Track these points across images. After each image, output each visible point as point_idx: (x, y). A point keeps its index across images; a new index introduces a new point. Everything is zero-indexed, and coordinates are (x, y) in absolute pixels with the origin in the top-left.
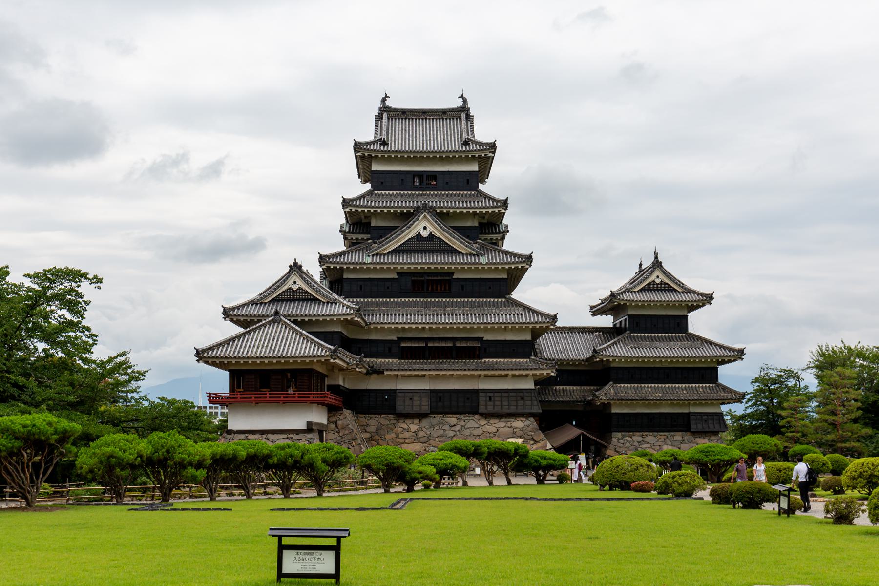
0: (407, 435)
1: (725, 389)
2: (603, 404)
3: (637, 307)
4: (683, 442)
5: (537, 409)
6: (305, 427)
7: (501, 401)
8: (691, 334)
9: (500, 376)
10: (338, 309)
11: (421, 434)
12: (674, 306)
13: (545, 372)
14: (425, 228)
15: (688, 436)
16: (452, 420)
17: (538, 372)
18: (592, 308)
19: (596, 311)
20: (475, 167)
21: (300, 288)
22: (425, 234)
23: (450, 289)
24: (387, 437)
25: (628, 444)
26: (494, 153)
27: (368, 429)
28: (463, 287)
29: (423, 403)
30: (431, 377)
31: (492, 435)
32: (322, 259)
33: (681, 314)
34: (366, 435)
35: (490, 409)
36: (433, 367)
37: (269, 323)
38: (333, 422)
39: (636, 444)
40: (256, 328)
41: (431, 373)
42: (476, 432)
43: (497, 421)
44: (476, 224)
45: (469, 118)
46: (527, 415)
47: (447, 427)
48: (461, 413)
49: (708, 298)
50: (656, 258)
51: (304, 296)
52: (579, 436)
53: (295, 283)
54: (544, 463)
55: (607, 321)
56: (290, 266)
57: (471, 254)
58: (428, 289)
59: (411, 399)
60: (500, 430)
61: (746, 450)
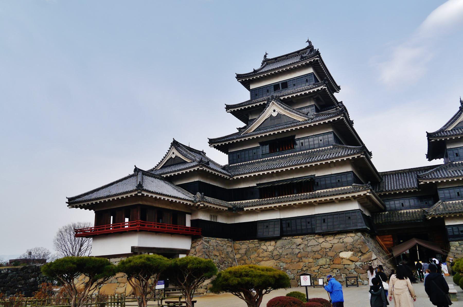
0: (265, 254)
2: (433, 218)
6: (129, 251)
7: (333, 222)
14: (274, 111)
16: (298, 240)
17: (356, 194)
21: (176, 156)
22: (275, 114)
26: (320, 57)
29: (276, 229)
31: (328, 250)
32: (212, 142)
34: (238, 256)
35: (324, 228)
41: (275, 205)
42: (315, 249)
43: (332, 238)
46: (356, 231)
47: (294, 246)
51: (180, 161)
52: (415, 246)
53: (173, 153)
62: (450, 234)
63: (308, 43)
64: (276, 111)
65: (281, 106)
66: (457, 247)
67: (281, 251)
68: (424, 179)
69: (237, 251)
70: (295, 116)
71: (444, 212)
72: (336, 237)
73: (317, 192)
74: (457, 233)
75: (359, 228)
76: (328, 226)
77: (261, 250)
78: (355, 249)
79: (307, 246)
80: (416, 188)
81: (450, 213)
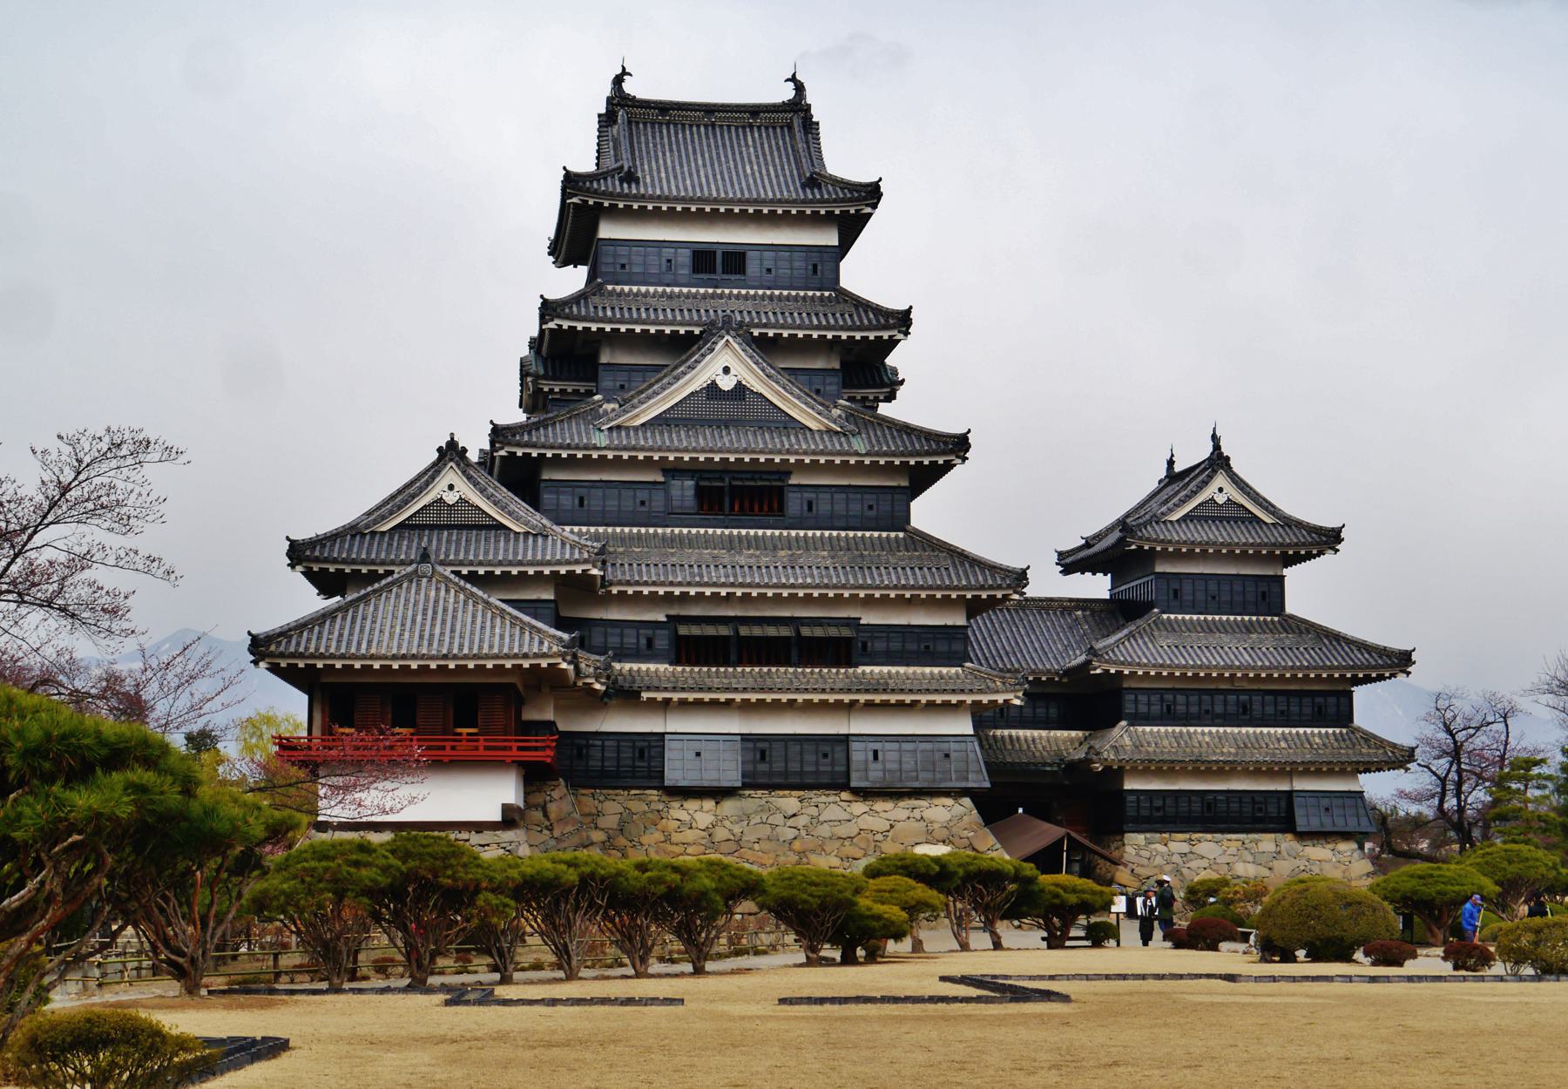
1: (1368, 738)
2: (1108, 769)
3: (1178, 556)
4: (1278, 854)
5: (980, 780)
6: (497, 817)
8: (1292, 617)
9: (901, 705)
10: (552, 550)
11: (721, 834)
12: (1257, 554)
13: (1000, 698)
14: (726, 370)
15: (1287, 842)
16: (789, 802)
17: (985, 699)
18: (1061, 555)
19: (1071, 563)
20: (831, 238)
22: (726, 384)
23: (781, 509)
24: (644, 840)
25: (1159, 860)
26: (875, 206)
27: (602, 822)
28: (810, 504)
30: (747, 707)
31: (879, 837)
33: (1271, 573)
36: (750, 683)
37: (409, 578)
38: (536, 807)
39: (1176, 859)
40: (381, 589)
42: (842, 831)
43: (889, 805)
44: (837, 365)
45: (810, 127)
48: (810, 787)
49: (1330, 539)
50: (1217, 447)
51: (475, 519)
52: (1062, 840)
53: (451, 487)
54: (1073, 899)
55: (1097, 586)
56: (440, 450)
57: (829, 431)
58: (732, 509)
59: (698, 754)
60: (898, 826)
61: (1499, 876)
62: (1131, 812)
63: (791, 85)
64: (733, 372)
65: (756, 363)
66: (1138, 848)
67: (737, 830)
68: (1107, 662)
69: (589, 819)
70: (795, 406)
71: (1136, 757)
72: (901, 804)
73: (860, 670)
74: (1145, 813)
75: (971, 785)
76: (884, 771)
77: (674, 825)
78: (955, 840)
79: (816, 820)
80: (1057, 673)
81: (1150, 761)
